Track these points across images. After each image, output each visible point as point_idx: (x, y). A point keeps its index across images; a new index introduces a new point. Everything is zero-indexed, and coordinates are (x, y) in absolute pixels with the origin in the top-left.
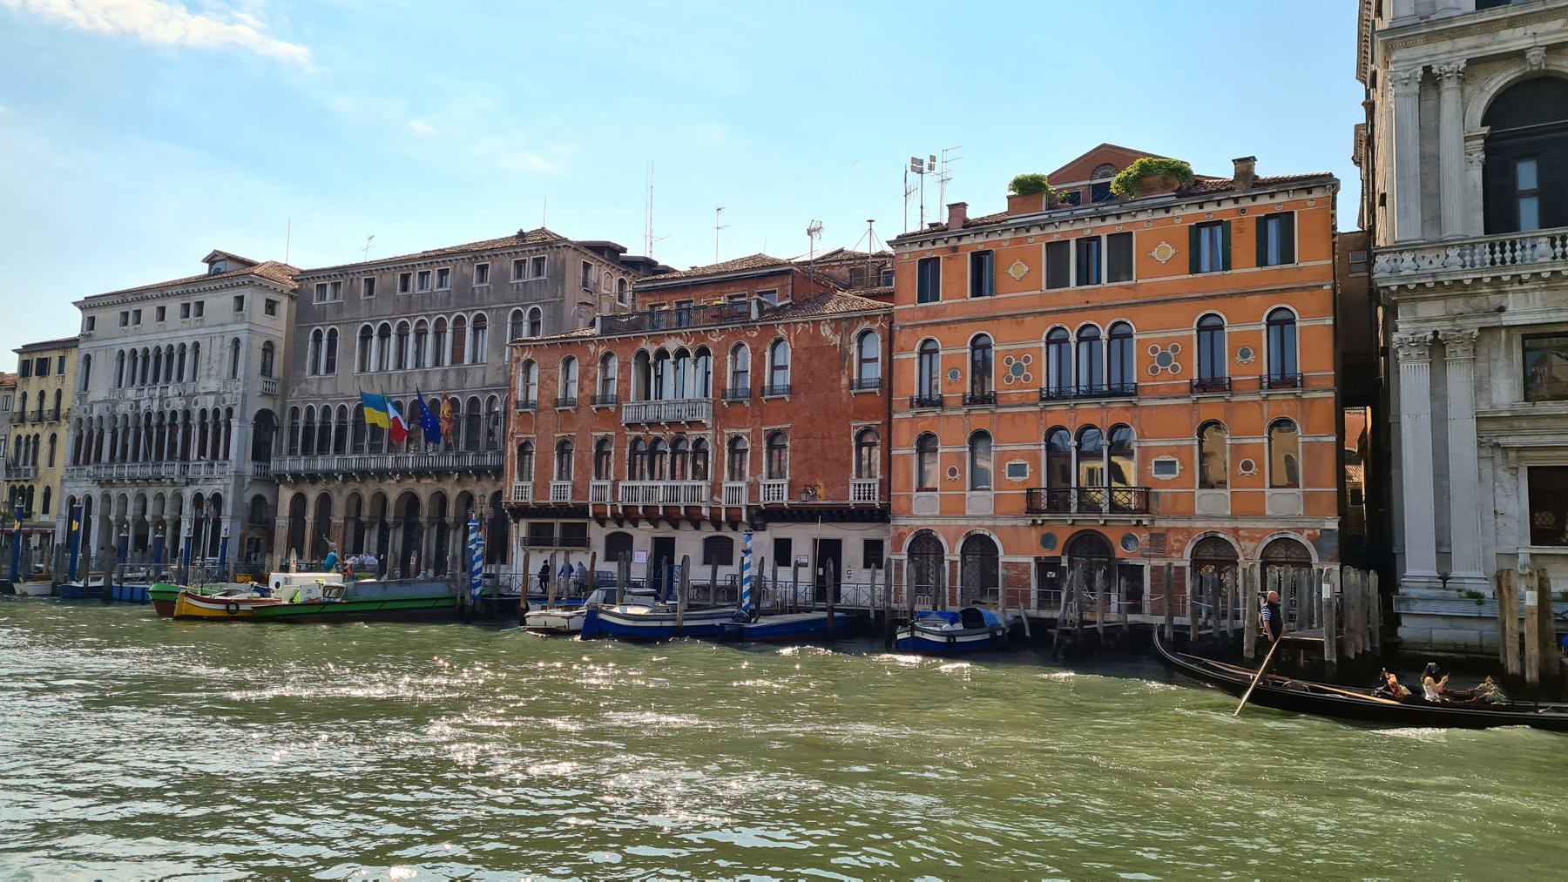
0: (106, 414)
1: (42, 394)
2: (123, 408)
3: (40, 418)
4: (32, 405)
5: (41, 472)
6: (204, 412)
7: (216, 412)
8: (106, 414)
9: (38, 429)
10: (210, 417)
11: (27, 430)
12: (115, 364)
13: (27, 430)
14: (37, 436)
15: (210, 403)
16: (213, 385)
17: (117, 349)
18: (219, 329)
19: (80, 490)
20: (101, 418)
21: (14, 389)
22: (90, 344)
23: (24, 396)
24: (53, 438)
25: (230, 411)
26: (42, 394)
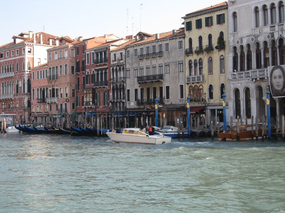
0: (252, 43)
1: (200, 38)
3: (200, 51)
4: (195, 45)
5: (206, 77)
8: (252, 43)
9: (201, 56)
11: (194, 57)
12: (253, 15)
13: (194, 57)
14: (200, 59)
17: (253, 8)
19: (241, 86)
20: (249, 46)
21: (184, 38)
22: (235, 6)
23: (190, 40)
24: (210, 61)
26: (200, 38)
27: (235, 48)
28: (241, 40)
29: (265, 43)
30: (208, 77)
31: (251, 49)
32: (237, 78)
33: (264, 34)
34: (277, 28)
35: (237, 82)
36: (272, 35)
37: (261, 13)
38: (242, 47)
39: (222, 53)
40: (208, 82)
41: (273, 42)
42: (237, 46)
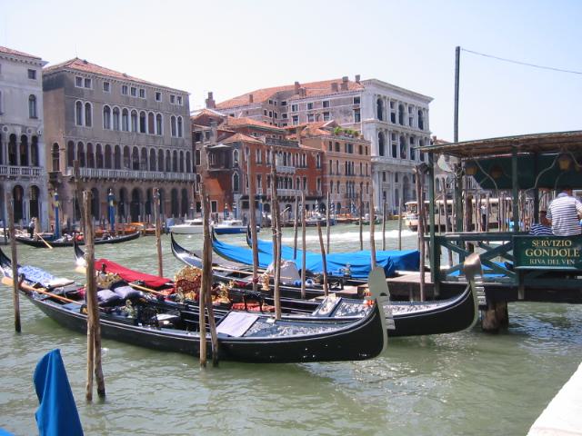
6: (13, 137)
7: (24, 138)
10: (19, 141)
15: (19, 132)
16: (17, 120)
25: (35, 139)
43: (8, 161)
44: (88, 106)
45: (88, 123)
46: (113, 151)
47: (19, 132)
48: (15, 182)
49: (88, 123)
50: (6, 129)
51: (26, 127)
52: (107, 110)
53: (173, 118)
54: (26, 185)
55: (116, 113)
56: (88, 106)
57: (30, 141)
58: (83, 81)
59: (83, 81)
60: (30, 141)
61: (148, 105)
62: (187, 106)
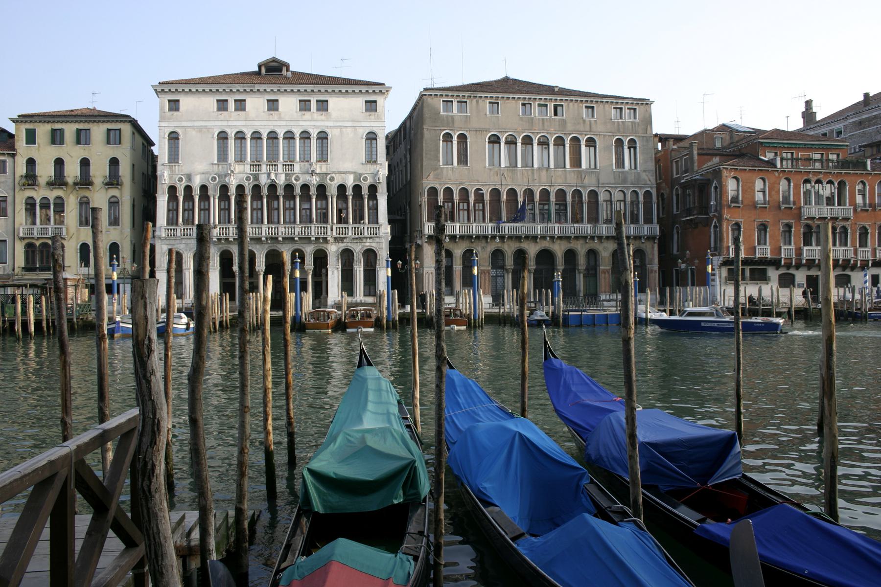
2: (233, 183)
6: (342, 188)
7: (357, 188)
15: (350, 182)
16: (348, 166)
18: (350, 124)
20: (204, 188)
25: (373, 189)
27: (172, 189)
28: (189, 177)
29: (240, 188)
30: (78, 231)
31: (210, 193)
32: (179, 234)
33: (239, 174)
34: (264, 168)
35: (178, 241)
36: (256, 178)
37: (231, 143)
38: (188, 189)
39: (114, 192)
40: (78, 238)
41: (257, 188)
42: (178, 186)
43: (335, 221)
44: (463, 138)
45: (463, 159)
46: (585, 198)
47: (350, 182)
48: (342, 246)
49: (463, 159)
50: (332, 179)
51: (360, 175)
52: (495, 140)
53: (619, 142)
54: (358, 249)
55: (511, 142)
56: (463, 138)
57: (365, 192)
58: (455, 104)
59: (455, 104)
60: (365, 192)
61: (570, 127)
62: (648, 121)
